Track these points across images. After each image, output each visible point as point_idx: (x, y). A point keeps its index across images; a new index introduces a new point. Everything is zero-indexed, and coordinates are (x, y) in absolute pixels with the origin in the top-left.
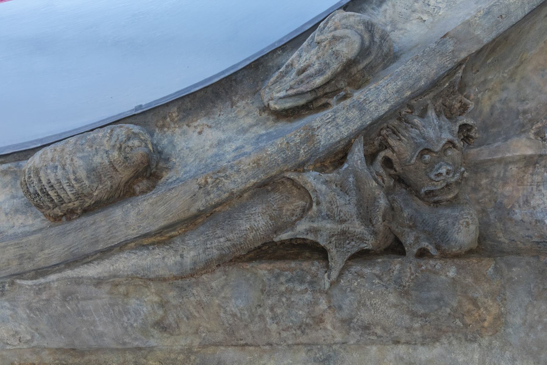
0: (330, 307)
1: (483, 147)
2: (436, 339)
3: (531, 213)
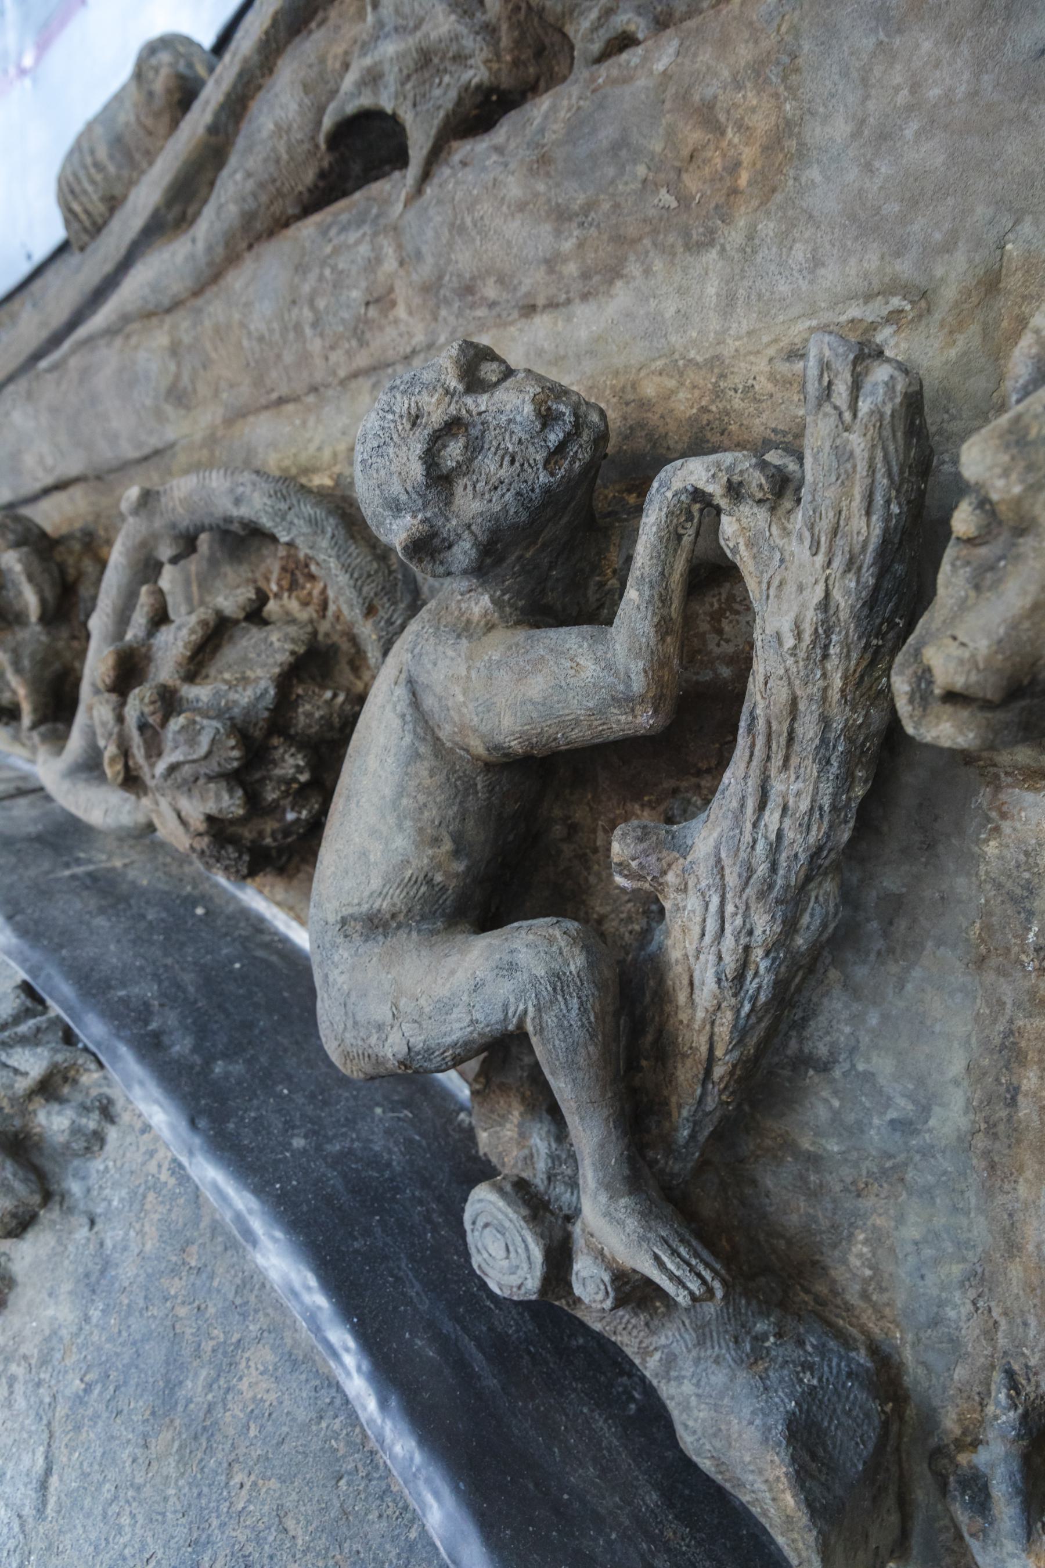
0: (401, 263)
2: (613, 273)
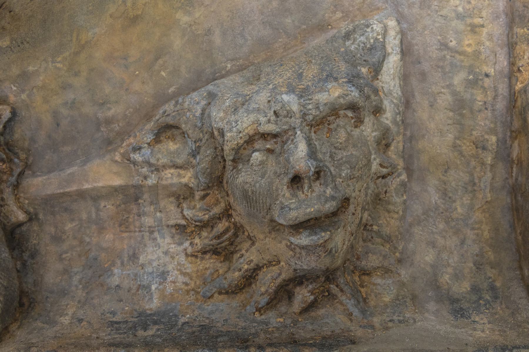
1: (52, 175)
3: (136, 275)
